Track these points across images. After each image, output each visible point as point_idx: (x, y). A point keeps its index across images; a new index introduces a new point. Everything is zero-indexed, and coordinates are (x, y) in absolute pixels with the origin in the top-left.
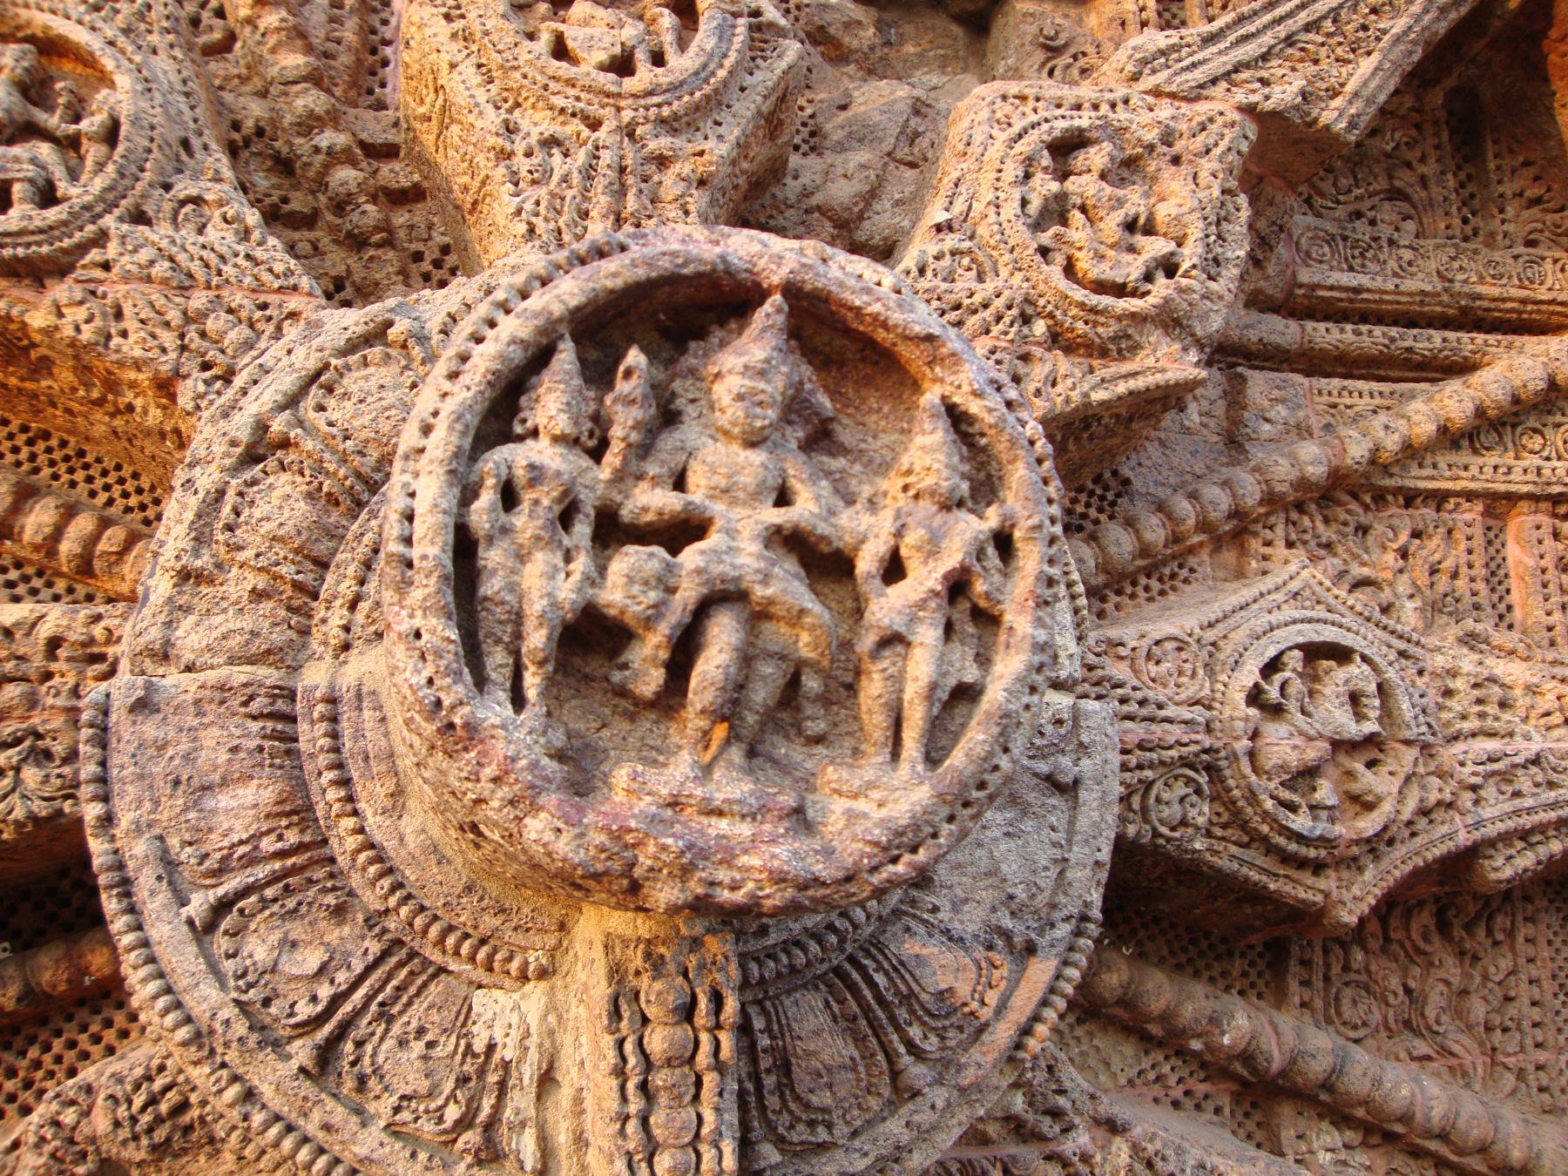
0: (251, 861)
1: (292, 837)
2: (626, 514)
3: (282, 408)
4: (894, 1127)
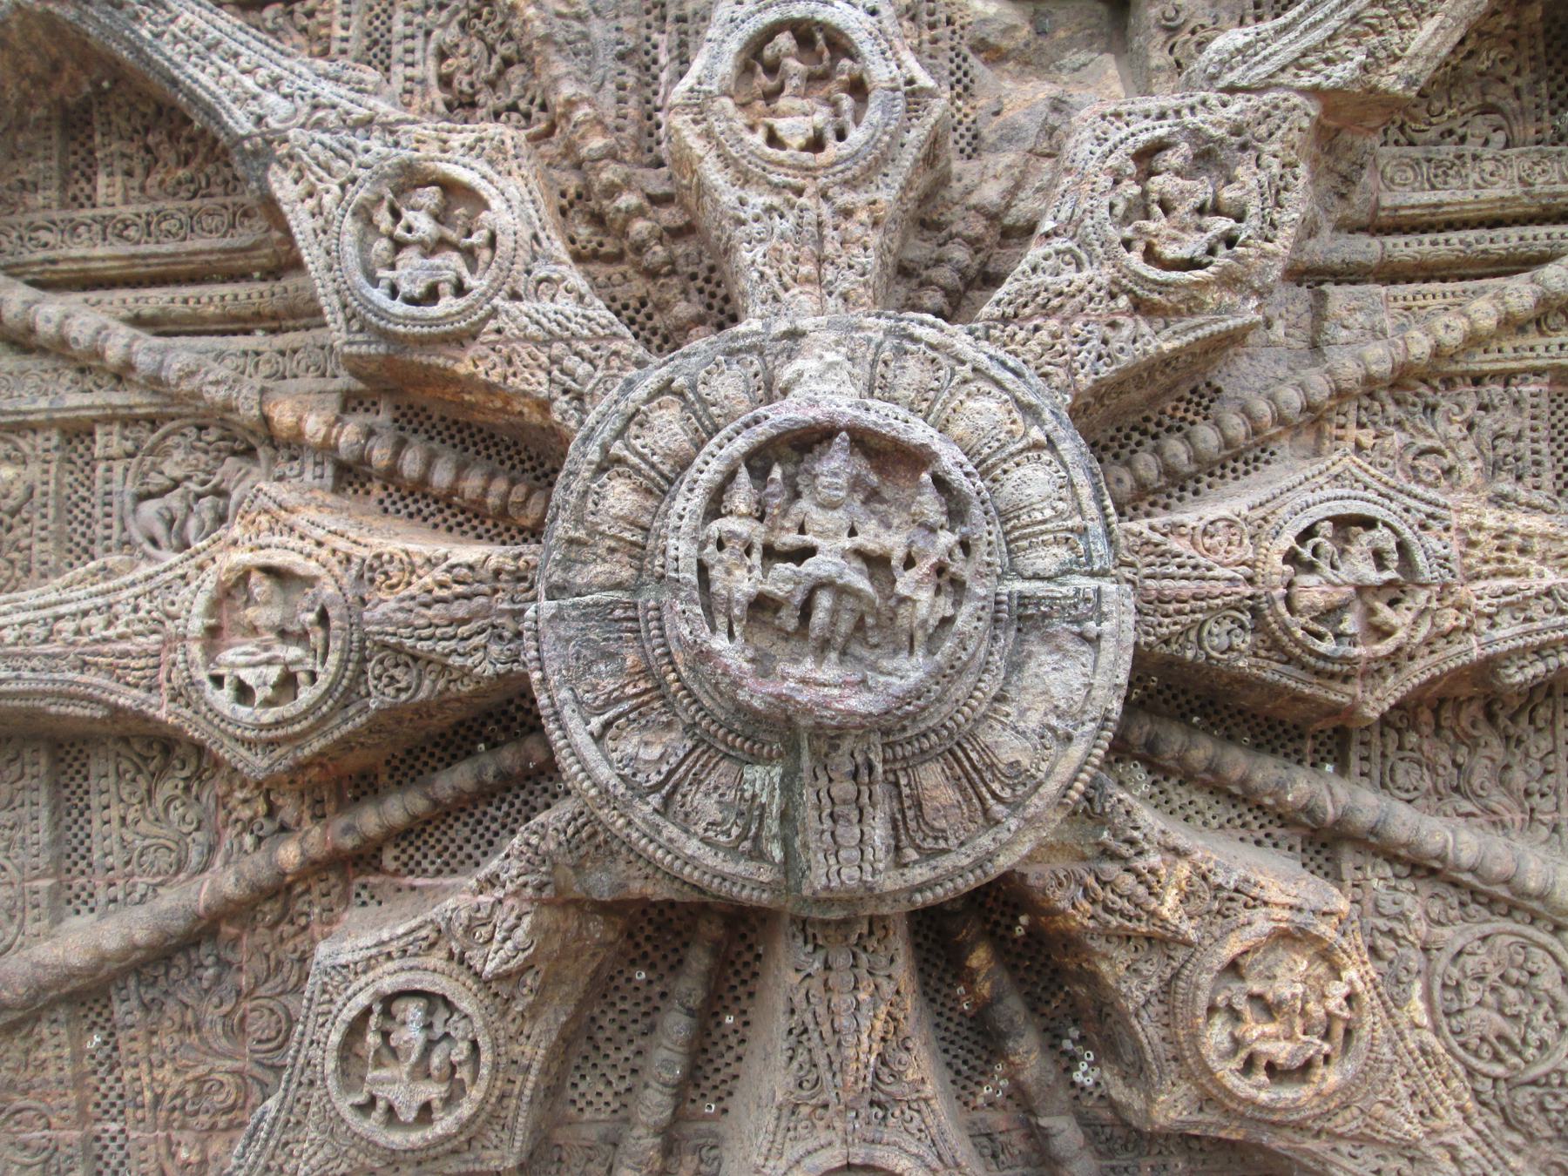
0: (618, 701)
1: (642, 685)
2: (778, 545)
3: (615, 438)
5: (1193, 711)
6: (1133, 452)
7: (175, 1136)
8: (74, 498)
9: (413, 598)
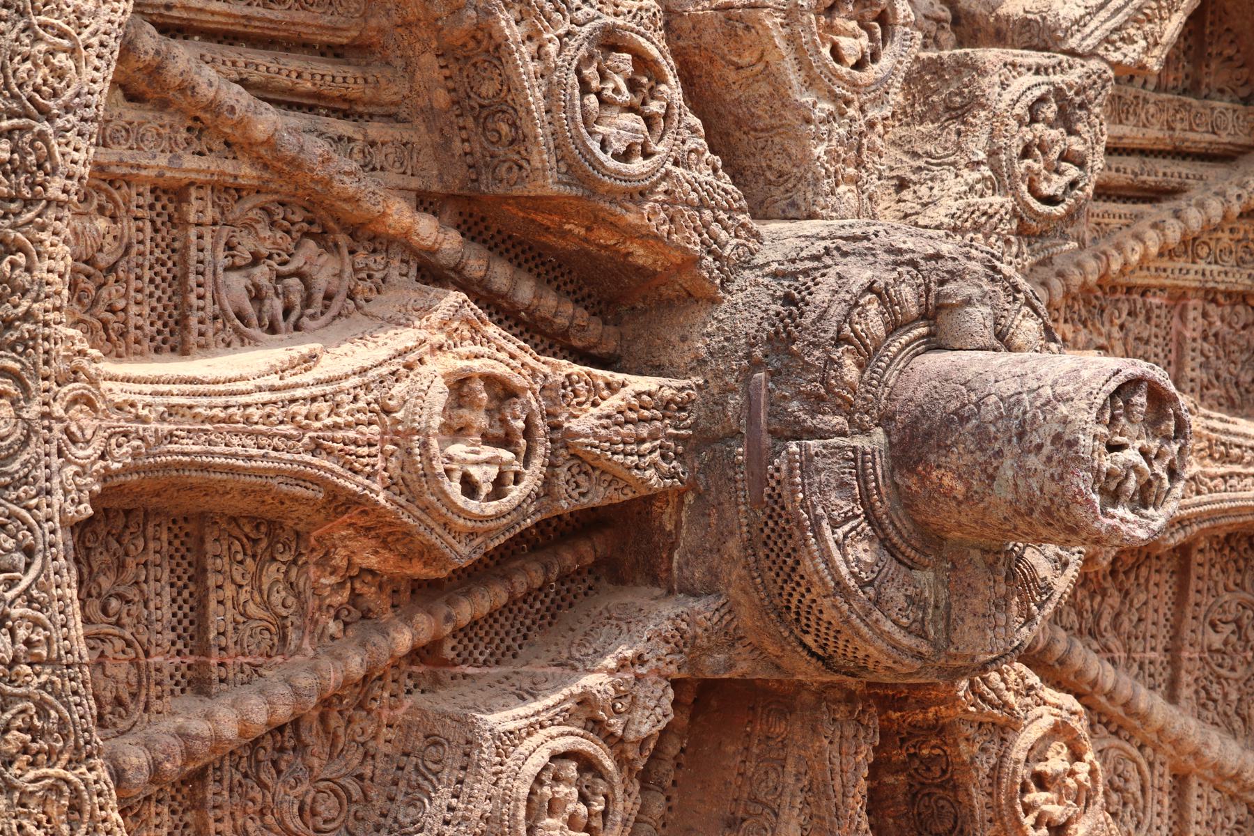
9: (608, 417)
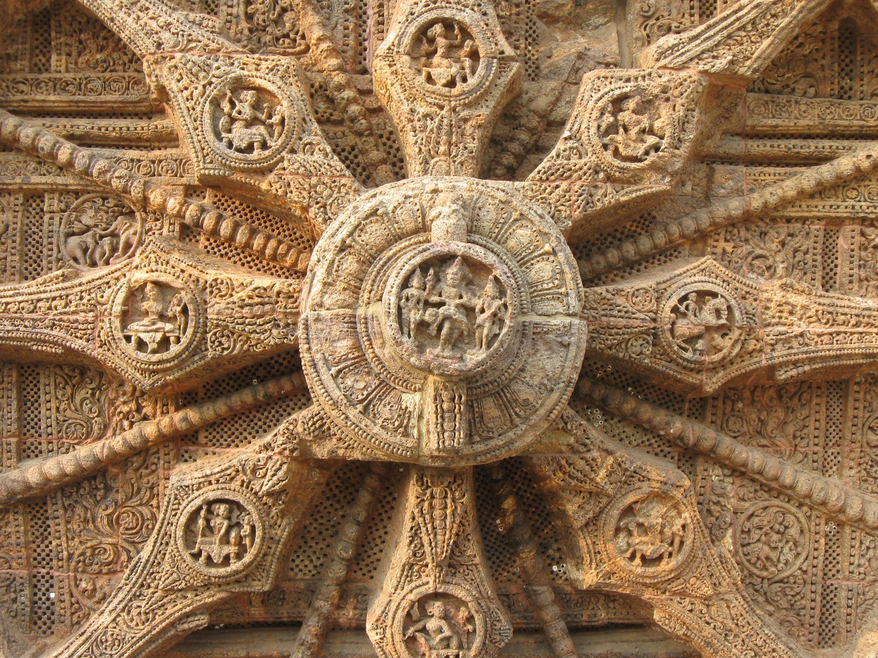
0: (345, 360)
1: (356, 354)
4: (511, 434)
5: (628, 385)
6: (608, 247)
7: (79, 576)
8: (30, 232)
